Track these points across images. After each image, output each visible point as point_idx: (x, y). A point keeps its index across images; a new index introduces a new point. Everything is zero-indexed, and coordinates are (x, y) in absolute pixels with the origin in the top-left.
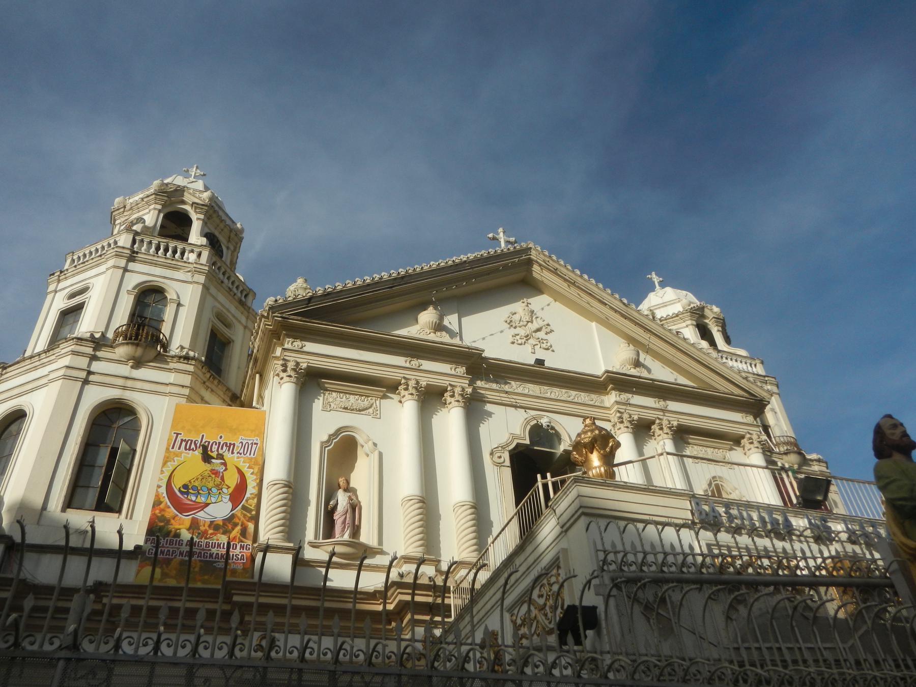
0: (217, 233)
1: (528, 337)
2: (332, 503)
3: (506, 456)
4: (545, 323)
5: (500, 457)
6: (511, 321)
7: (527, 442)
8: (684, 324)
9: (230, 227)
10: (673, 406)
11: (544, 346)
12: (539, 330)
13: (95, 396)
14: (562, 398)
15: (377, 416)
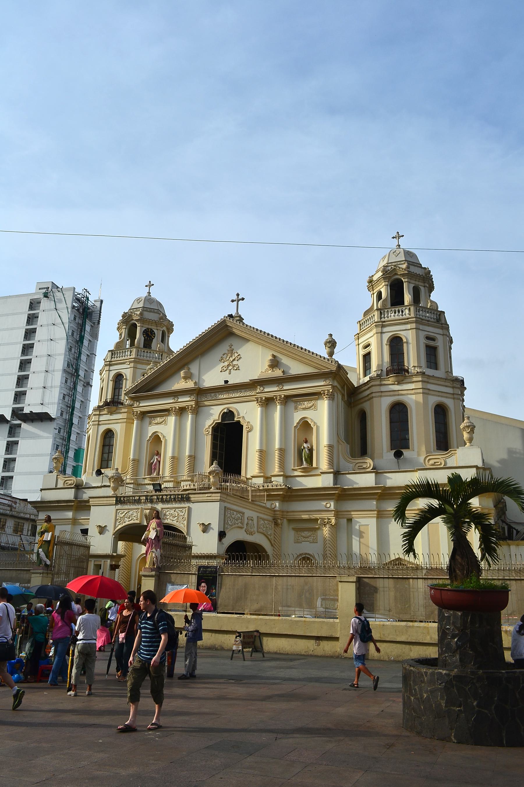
0: (150, 327)
1: (228, 366)
3: (210, 430)
4: (238, 354)
5: (207, 431)
6: (222, 360)
7: (220, 421)
8: (381, 286)
9: (154, 320)
12: (234, 360)
13: (102, 428)
14: (238, 396)
15: (166, 424)
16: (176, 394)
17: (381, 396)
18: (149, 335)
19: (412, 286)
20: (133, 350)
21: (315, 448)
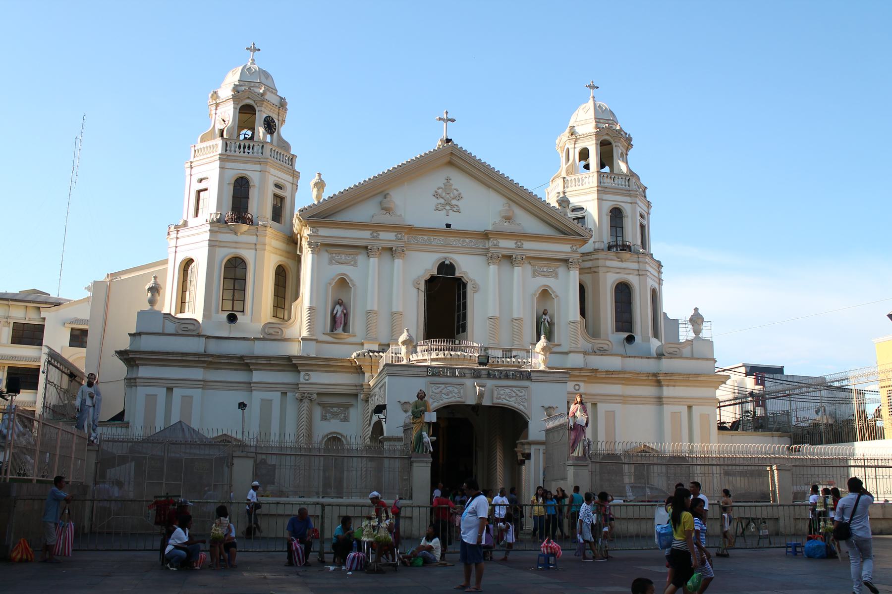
0: (271, 115)
2: (335, 312)
5: (419, 284)
10: (527, 245)
11: (454, 209)
15: (355, 264)
16: (374, 227)
17: (607, 272)
18: (270, 126)
19: (620, 151)
20: (263, 146)
21: (556, 321)
